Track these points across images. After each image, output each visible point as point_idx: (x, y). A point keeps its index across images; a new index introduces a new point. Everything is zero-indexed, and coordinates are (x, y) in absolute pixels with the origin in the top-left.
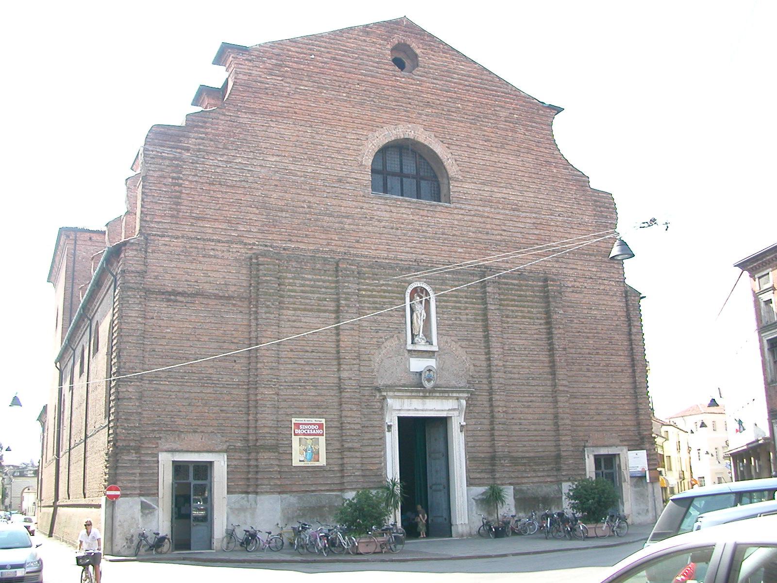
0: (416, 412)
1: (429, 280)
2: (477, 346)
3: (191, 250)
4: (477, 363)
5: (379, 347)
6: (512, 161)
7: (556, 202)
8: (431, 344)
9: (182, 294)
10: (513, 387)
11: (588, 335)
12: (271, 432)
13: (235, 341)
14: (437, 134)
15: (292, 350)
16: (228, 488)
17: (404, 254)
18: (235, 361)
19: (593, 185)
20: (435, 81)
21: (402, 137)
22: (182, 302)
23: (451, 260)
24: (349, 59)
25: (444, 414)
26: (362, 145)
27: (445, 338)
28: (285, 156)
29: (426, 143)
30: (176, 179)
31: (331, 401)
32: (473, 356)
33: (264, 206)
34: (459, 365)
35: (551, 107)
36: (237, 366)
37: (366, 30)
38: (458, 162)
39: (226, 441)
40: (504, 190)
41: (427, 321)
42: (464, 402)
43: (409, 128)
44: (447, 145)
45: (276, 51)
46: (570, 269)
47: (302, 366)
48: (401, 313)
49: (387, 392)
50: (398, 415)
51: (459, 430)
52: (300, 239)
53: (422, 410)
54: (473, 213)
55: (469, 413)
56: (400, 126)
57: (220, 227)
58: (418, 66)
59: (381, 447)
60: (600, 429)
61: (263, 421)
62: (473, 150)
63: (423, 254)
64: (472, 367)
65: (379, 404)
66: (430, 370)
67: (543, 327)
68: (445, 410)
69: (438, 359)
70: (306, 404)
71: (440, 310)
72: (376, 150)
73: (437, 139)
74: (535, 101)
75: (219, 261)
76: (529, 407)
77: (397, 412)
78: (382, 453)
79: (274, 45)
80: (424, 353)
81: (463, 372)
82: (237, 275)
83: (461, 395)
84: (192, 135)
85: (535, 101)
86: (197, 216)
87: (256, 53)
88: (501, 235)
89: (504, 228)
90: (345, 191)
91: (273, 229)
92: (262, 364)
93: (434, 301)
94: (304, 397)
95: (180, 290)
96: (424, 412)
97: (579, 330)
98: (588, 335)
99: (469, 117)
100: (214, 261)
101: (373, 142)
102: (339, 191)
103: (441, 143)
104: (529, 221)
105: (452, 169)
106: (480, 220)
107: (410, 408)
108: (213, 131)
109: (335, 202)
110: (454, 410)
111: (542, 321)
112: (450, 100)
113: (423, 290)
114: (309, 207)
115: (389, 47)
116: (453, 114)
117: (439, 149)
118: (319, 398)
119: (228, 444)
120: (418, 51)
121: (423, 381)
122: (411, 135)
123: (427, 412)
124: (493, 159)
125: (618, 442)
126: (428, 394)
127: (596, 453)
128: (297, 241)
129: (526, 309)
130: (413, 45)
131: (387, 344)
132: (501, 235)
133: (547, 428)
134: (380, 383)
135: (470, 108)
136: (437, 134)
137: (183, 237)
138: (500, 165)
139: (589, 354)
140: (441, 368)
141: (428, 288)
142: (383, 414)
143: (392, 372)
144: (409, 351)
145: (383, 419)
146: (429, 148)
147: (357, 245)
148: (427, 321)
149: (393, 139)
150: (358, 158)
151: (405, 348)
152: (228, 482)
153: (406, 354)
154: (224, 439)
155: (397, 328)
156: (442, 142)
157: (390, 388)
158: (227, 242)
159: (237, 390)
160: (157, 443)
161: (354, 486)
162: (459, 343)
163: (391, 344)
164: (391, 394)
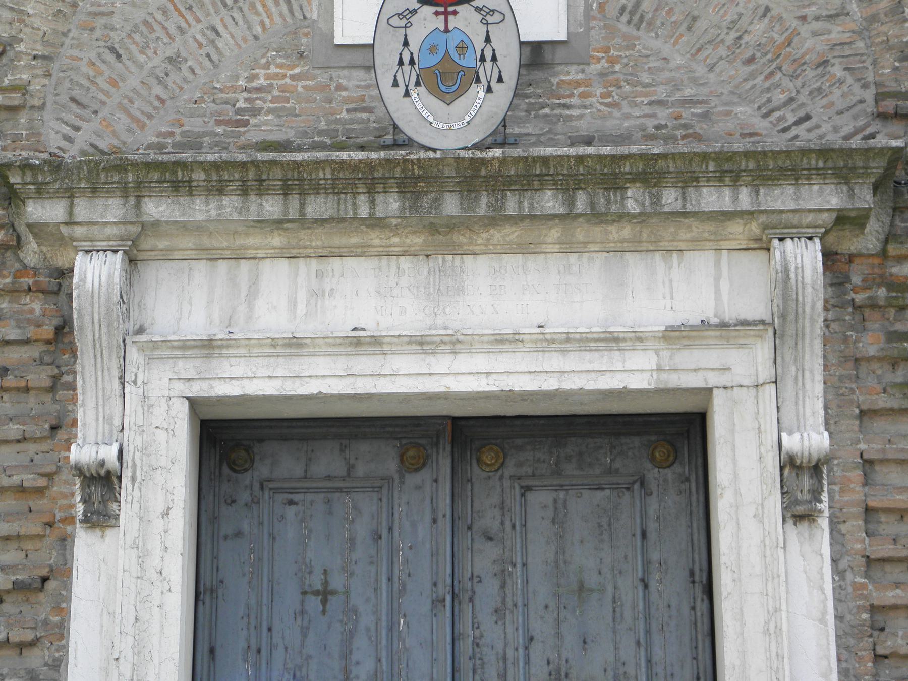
0: (365, 363)
49: (70, 194)
50: (198, 390)
51: (775, 503)
65: (36, 305)
68: (639, 338)
77: (187, 368)
81: (837, 32)
96: (442, 363)
107: (306, 329)
121: (393, 97)
123: (463, 362)
126: (451, 205)
134: (54, 142)
143: (174, 61)
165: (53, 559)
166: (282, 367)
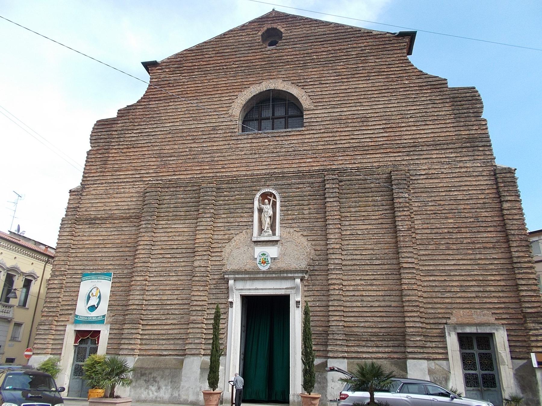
0: (257, 291)
1: (276, 188)
2: (318, 233)
3: (110, 190)
4: (319, 248)
5: (230, 240)
6: (362, 85)
7: (408, 107)
8: (274, 234)
9: (99, 219)
10: (355, 267)
11: (448, 215)
12: (137, 308)
13: (128, 245)
14: (293, 82)
15: (162, 249)
16: (107, 350)
17: (261, 170)
18: (127, 259)
19: (451, 84)
20: (295, 46)
21: (265, 89)
22: (98, 224)
23: (300, 169)
24: (228, 50)
25: (282, 292)
26: (234, 102)
27: (288, 230)
28: (177, 122)
29: (284, 89)
30: (107, 149)
31: (187, 284)
32: (313, 243)
33: (160, 156)
34: (301, 250)
35: (402, 35)
36: (127, 262)
37: (243, 28)
38: (311, 97)
39: (113, 316)
40: (354, 108)
41: (273, 218)
42: (298, 281)
43: (271, 83)
44: (302, 87)
45: (178, 59)
46: (423, 159)
47: (169, 260)
48: (250, 214)
52: (182, 173)
53: (262, 289)
54: (322, 131)
55: (308, 292)
56: (263, 83)
57: (130, 173)
58: (281, 40)
59: (226, 320)
60: (467, 306)
61: (133, 301)
62: (324, 85)
63: (275, 168)
64: (313, 251)
66: (264, 254)
67: (388, 211)
68: (283, 289)
69: (281, 247)
70: (168, 288)
71: (283, 208)
72: (244, 103)
73: (294, 85)
74: (388, 35)
75: (127, 195)
76: (371, 285)
77: (240, 291)
78: (226, 325)
79: (177, 55)
80: (268, 243)
81: (304, 256)
82: (136, 202)
83: (296, 275)
84: (119, 122)
85: (388, 35)
86: (117, 169)
87: (164, 64)
88: (350, 143)
89: (352, 137)
90: (217, 136)
91: (164, 169)
92: (139, 259)
93: (279, 201)
94: (168, 282)
95: (99, 216)
96: (264, 291)
97: (435, 212)
98: (448, 215)
99: (322, 63)
100: (123, 195)
101: (242, 98)
102: (213, 136)
103: (297, 87)
104: (378, 127)
105: (305, 102)
106: (330, 135)
108: (133, 117)
109: (209, 144)
110: (291, 288)
111: (387, 207)
112: (306, 55)
113: (271, 194)
114: (190, 151)
115: (260, 34)
116: (309, 64)
117: (295, 91)
118: (179, 283)
119: (113, 317)
120: (282, 30)
122: (272, 87)
123: (266, 291)
124: (343, 88)
125: (492, 320)
127: (460, 331)
128: (179, 174)
129: (370, 199)
130: (279, 27)
131: (236, 238)
132: (350, 143)
133: (393, 304)
135: (324, 56)
136: (293, 82)
137: (105, 183)
138: (349, 91)
139: (449, 232)
140: (283, 255)
141: (274, 192)
142: (228, 293)
144: (255, 242)
145: (228, 297)
146: (288, 92)
147: (222, 170)
148: (273, 218)
149: (257, 92)
150: (229, 111)
151: (251, 240)
152: (107, 346)
153: (253, 244)
154: (112, 314)
155: (246, 225)
156: (298, 85)
157: (235, 272)
158: (132, 182)
159: (126, 279)
160: (69, 318)
161: (193, 352)
162: (301, 233)
163: (240, 238)
164: (232, 276)
165: (227, 310)
166: (249, 291)
